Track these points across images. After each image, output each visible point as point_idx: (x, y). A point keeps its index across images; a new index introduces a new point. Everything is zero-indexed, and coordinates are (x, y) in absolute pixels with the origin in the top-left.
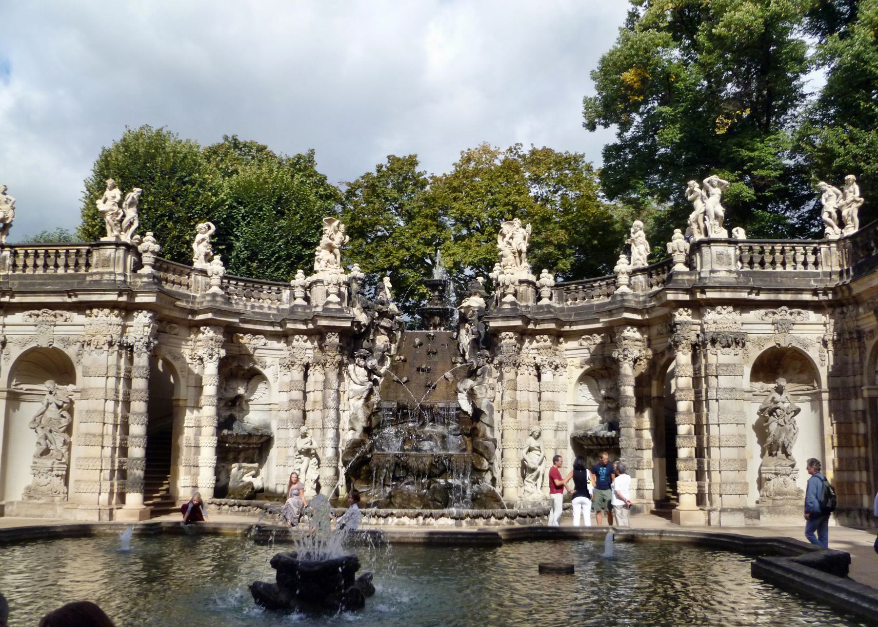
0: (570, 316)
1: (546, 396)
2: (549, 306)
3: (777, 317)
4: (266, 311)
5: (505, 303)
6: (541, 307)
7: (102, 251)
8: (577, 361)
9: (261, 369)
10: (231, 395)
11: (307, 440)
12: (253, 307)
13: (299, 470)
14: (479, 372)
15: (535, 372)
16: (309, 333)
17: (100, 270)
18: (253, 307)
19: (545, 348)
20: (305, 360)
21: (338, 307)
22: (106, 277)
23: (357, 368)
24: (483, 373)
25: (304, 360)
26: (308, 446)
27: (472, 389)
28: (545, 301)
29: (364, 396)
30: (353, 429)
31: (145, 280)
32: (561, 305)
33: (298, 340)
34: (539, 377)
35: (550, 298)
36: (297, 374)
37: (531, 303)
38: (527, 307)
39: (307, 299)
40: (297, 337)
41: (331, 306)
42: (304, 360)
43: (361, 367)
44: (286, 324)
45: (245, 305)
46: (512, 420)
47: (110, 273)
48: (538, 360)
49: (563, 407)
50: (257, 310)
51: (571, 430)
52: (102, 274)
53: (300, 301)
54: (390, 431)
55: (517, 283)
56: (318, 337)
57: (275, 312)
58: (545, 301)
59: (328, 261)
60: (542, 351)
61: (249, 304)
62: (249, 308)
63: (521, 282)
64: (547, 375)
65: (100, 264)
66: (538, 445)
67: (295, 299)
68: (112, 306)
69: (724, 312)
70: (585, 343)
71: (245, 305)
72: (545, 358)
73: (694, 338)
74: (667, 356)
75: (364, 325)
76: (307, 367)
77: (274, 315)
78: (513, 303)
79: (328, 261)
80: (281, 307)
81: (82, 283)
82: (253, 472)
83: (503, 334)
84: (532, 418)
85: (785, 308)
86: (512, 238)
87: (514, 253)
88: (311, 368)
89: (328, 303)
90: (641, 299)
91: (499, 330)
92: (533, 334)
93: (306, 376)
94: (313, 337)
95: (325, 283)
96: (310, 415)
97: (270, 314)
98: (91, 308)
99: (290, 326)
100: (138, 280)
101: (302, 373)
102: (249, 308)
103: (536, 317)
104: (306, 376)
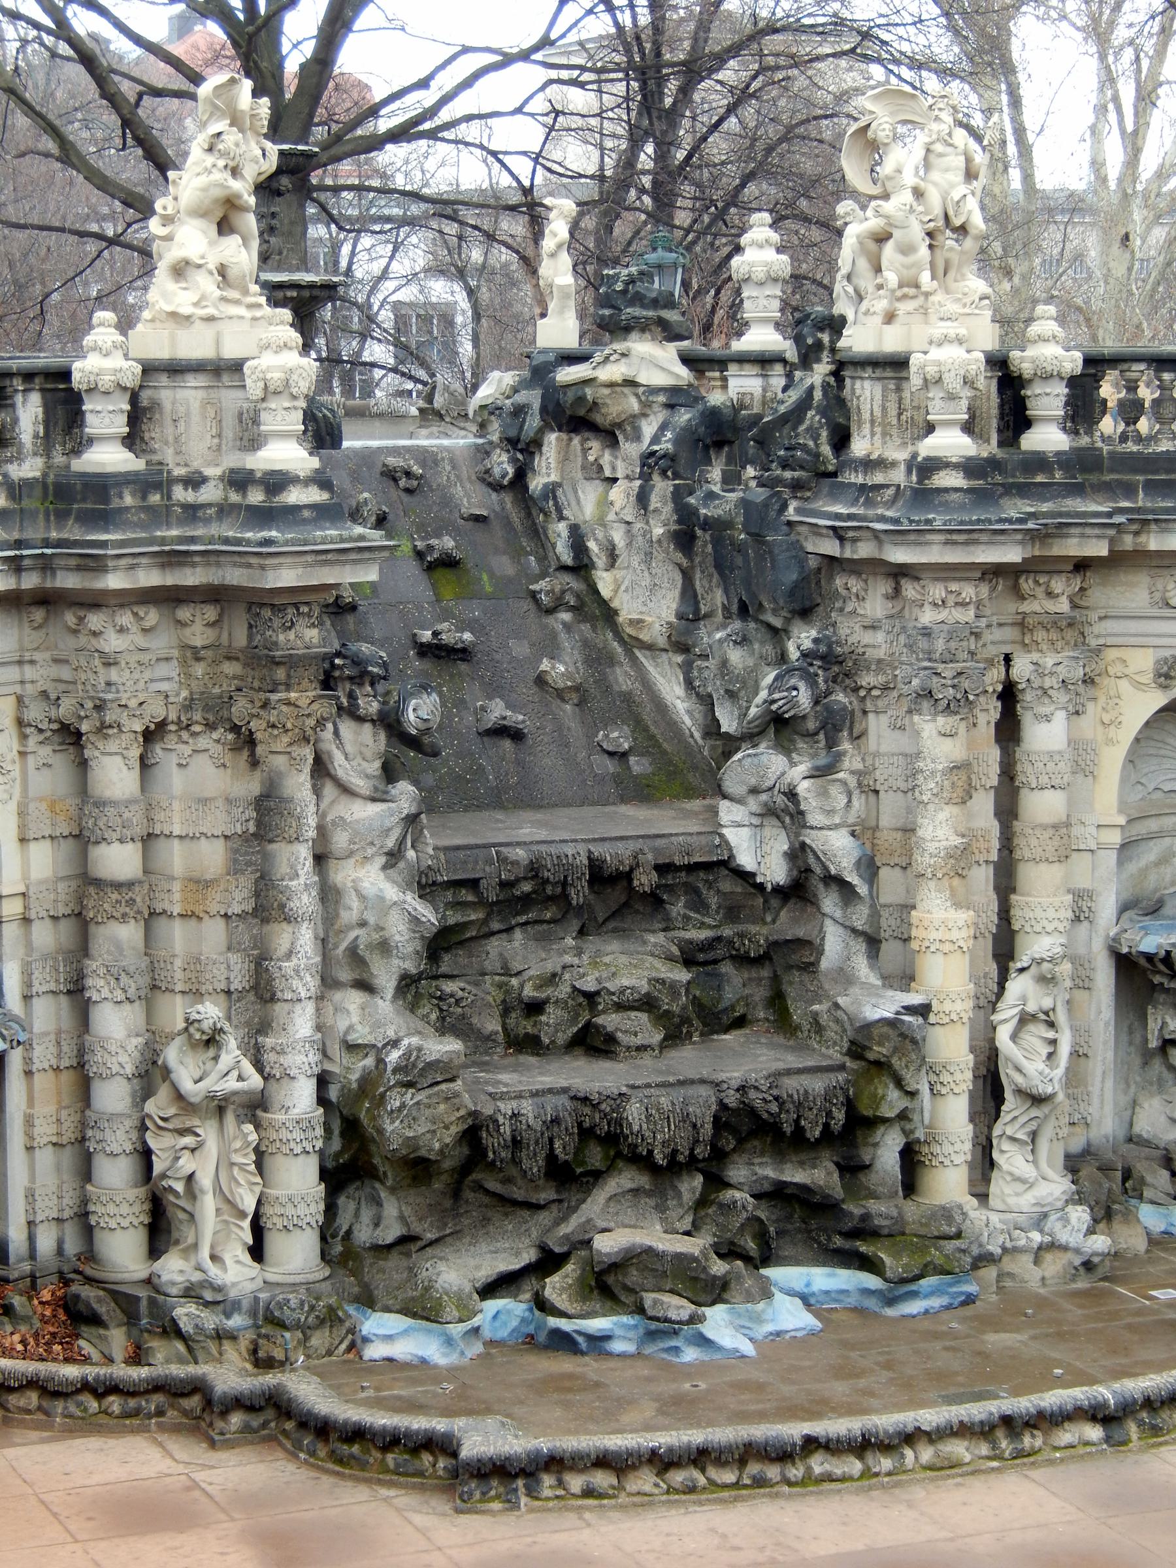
6: (1039, 462)
13: (190, 1178)
21: (315, 495)
39: (133, 440)
60: (1040, 635)
66: (1047, 1003)
78: (970, 467)
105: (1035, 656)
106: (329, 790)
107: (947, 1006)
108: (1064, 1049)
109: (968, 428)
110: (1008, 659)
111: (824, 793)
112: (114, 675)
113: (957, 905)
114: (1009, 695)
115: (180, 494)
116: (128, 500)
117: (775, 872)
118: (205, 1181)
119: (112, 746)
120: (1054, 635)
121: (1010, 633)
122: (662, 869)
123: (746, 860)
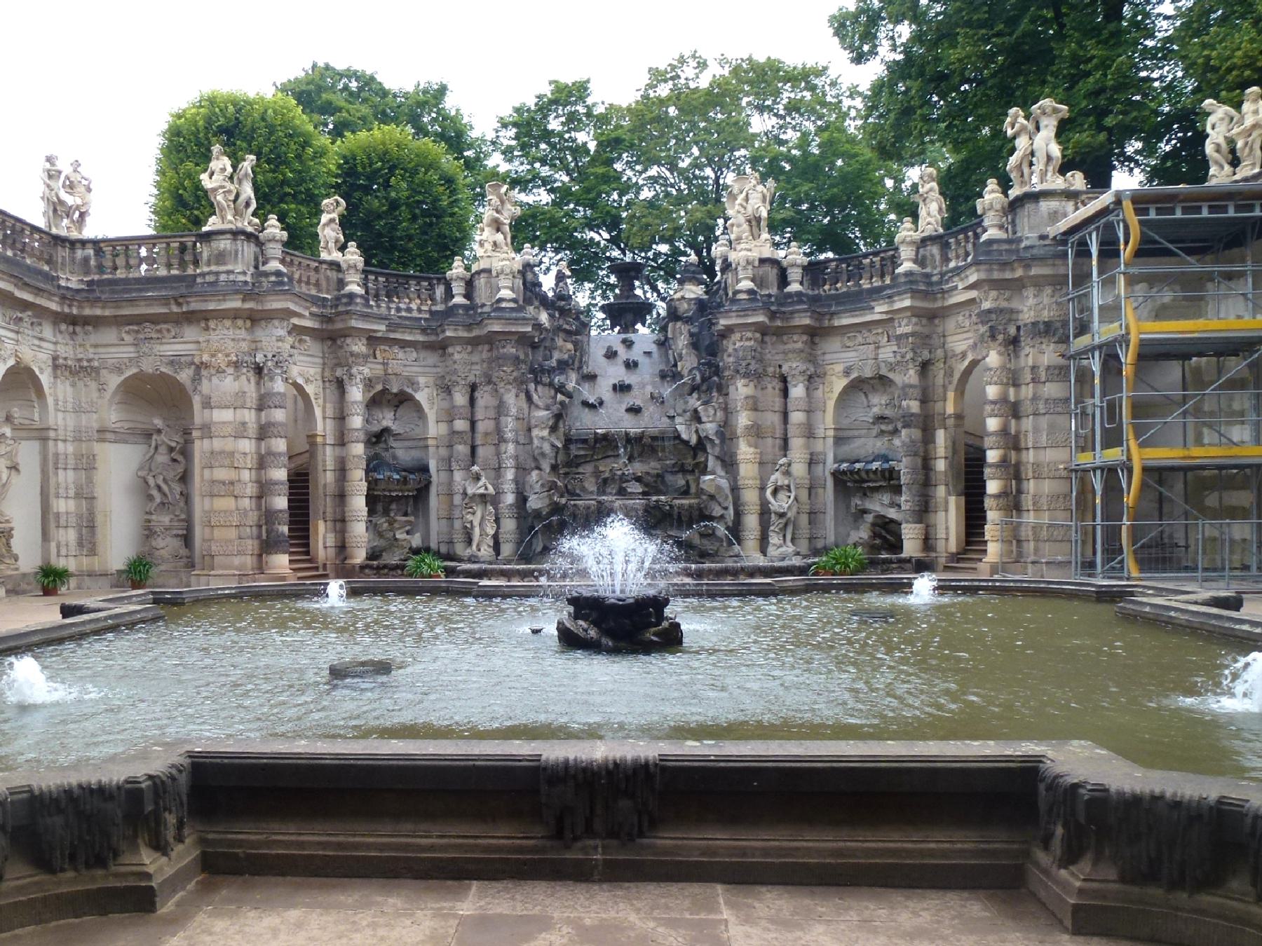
0: (830, 306)
1: (797, 417)
2: (799, 294)
4: (415, 314)
5: (740, 292)
6: (790, 295)
8: (839, 368)
9: (413, 393)
10: (376, 428)
11: (481, 483)
12: (398, 310)
13: (471, 522)
14: (704, 388)
15: (778, 385)
16: (474, 342)
18: (398, 310)
19: (794, 351)
20: (471, 379)
21: (512, 305)
23: (540, 388)
24: (709, 390)
25: (469, 379)
26: (482, 491)
27: (696, 411)
28: (794, 287)
29: (550, 423)
30: (538, 468)
32: (816, 292)
34: (785, 393)
35: (801, 283)
36: (460, 399)
37: (773, 290)
38: (770, 296)
39: (468, 296)
40: (459, 348)
41: (504, 305)
42: (469, 379)
43: (544, 385)
44: (443, 331)
45: (389, 308)
46: (752, 450)
48: (785, 369)
49: (820, 432)
50: (404, 314)
51: (831, 465)
53: (459, 300)
54: (588, 469)
55: (757, 263)
56: (487, 347)
57: (427, 316)
58: (794, 287)
59: (495, 244)
61: (393, 305)
62: (393, 312)
63: (763, 261)
64: (797, 391)
66: (786, 482)
67: (453, 297)
71: (389, 308)
72: (794, 365)
75: (546, 329)
76: (473, 388)
77: (426, 319)
78: (750, 292)
79: (495, 244)
80: (434, 308)
82: (408, 528)
83: (738, 336)
84: (777, 449)
86: (747, 199)
87: (749, 221)
89: (500, 300)
91: (729, 330)
92: (779, 333)
93: (472, 401)
94: (480, 348)
95: (494, 273)
96: (481, 452)
97: (421, 318)
99: (448, 334)
101: (467, 397)
102: (393, 312)
103: (783, 309)
104: (472, 401)
105: (790, 364)
106: (533, 407)
107: (746, 482)
108: (792, 498)
109: (753, 280)
110: (780, 366)
111: (706, 410)
112: (456, 366)
113: (750, 446)
114: (784, 380)
115: (479, 310)
116: (461, 312)
117: (694, 440)
118: (476, 523)
119: (457, 389)
120: (795, 355)
121: (780, 356)
122: (654, 438)
123: (684, 436)
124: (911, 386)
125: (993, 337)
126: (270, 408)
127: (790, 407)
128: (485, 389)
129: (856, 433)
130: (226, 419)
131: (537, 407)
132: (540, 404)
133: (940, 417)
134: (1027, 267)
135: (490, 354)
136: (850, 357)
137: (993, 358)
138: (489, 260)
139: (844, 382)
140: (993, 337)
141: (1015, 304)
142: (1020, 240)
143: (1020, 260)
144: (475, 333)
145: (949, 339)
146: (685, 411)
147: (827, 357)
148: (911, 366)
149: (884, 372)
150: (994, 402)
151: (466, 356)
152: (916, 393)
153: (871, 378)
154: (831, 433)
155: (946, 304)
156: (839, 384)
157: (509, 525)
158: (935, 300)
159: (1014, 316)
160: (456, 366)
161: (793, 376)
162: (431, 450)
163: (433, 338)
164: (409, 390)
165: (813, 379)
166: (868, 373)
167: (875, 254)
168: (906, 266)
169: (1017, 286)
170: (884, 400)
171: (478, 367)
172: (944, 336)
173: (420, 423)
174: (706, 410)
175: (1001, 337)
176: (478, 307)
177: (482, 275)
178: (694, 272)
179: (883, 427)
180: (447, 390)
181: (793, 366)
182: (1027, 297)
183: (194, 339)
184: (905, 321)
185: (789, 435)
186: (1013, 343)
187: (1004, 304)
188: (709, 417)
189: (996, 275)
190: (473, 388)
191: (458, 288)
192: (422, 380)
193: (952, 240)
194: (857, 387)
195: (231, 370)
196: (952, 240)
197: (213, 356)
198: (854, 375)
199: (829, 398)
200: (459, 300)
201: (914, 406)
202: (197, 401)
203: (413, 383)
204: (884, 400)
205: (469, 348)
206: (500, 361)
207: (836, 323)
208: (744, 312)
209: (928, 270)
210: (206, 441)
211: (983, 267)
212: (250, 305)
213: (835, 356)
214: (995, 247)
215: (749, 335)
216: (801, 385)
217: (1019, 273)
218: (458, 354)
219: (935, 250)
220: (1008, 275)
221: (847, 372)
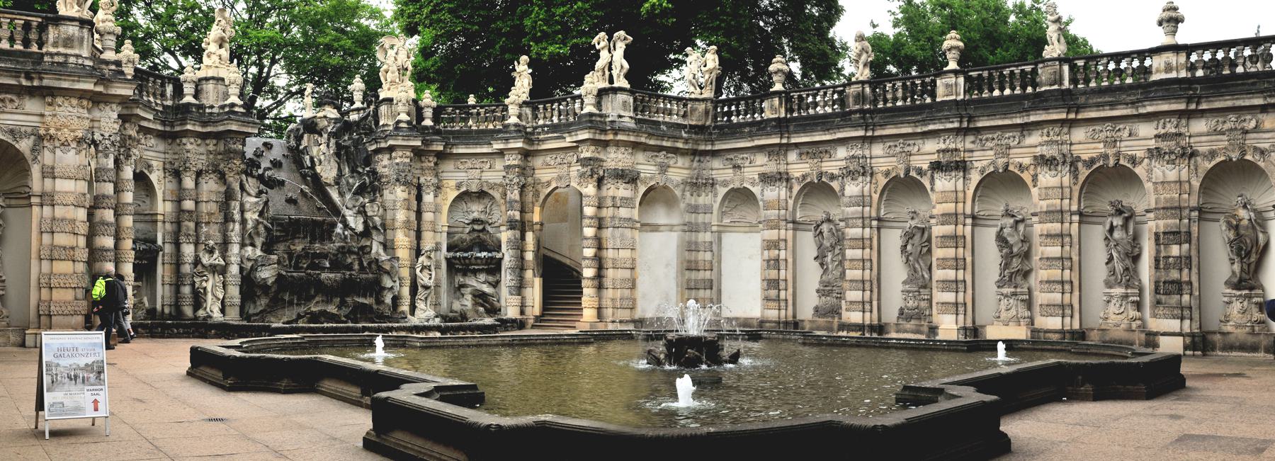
3: (658, 160)
7: (63, 28)
8: (453, 183)
9: (148, 174)
16: (204, 136)
17: (62, 50)
20: (200, 166)
21: (242, 110)
22: (72, 60)
23: (250, 179)
30: (253, 245)
31: (113, 67)
33: (191, 143)
41: (237, 109)
46: (407, 239)
47: (77, 56)
52: (66, 55)
60: (427, 172)
64: (428, 198)
65: (60, 42)
68: (82, 95)
69: (626, 153)
70: (461, 167)
73: (601, 173)
74: (553, 185)
81: (39, 64)
85: (665, 153)
88: (203, 176)
90: (528, 130)
94: (208, 142)
98: (53, 96)
99: (189, 127)
100: (104, 67)
106: (245, 194)
110: (419, 178)
112: (189, 155)
114: (419, 188)
115: (207, 110)
118: (209, 289)
119: (188, 174)
121: (419, 171)
124: (516, 201)
125: (592, 176)
126: (105, 181)
127: (424, 208)
128: (212, 176)
129: (456, 230)
130: (67, 190)
131: (249, 194)
132: (253, 193)
133: (530, 224)
134: (616, 134)
135: (215, 148)
136: (462, 176)
137: (590, 189)
138: (216, 69)
139: (456, 193)
140: (592, 176)
141: (602, 156)
142: (606, 116)
143: (612, 129)
144: (209, 129)
145: (536, 172)
146: (354, 207)
147: (444, 174)
148: (516, 187)
149: (485, 189)
150: (591, 218)
151: (196, 148)
152: (518, 206)
153: (475, 193)
154: (446, 229)
155: (540, 148)
156: (453, 194)
157: (234, 291)
158: (533, 144)
159: (601, 163)
160: (189, 155)
161: (428, 186)
162: (160, 224)
163: (168, 129)
164: (146, 172)
165: (438, 188)
166: (474, 189)
167: (482, 107)
168: (513, 120)
169: (605, 144)
170: (481, 208)
171: (204, 157)
172: (534, 169)
173: (148, 202)
174: (372, 207)
175: (596, 176)
176: (206, 107)
177: (211, 82)
178: (332, 98)
179: (476, 227)
180: (177, 175)
181: (427, 179)
182: (610, 153)
183: (39, 112)
184: (514, 156)
185: (423, 229)
186: (600, 182)
187: (597, 155)
188: (374, 212)
189: (598, 137)
190: (199, 174)
191: (188, 89)
192: (154, 163)
193: (541, 106)
194: (465, 197)
195: (74, 145)
196: (541, 106)
197: (58, 130)
198: (463, 189)
199: (445, 204)
200: (188, 99)
201: (517, 215)
202: (36, 171)
203: (149, 166)
204: (481, 208)
205: (199, 141)
206: (232, 155)
207: (455, 151)
208: (407, 137)
209: (524, 123)
210: (47, 210)
211: (592, 131)
212: (100, 89)
213: (450, 174)
214: (594, 118)
215: (408, 154)
216: (432, 194)
217: (610, 137)
218: (190, 145)
219: (528, 111)
220: (603, 137)
221: (458, 186)
